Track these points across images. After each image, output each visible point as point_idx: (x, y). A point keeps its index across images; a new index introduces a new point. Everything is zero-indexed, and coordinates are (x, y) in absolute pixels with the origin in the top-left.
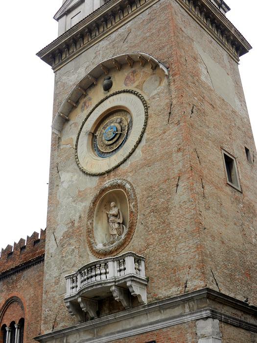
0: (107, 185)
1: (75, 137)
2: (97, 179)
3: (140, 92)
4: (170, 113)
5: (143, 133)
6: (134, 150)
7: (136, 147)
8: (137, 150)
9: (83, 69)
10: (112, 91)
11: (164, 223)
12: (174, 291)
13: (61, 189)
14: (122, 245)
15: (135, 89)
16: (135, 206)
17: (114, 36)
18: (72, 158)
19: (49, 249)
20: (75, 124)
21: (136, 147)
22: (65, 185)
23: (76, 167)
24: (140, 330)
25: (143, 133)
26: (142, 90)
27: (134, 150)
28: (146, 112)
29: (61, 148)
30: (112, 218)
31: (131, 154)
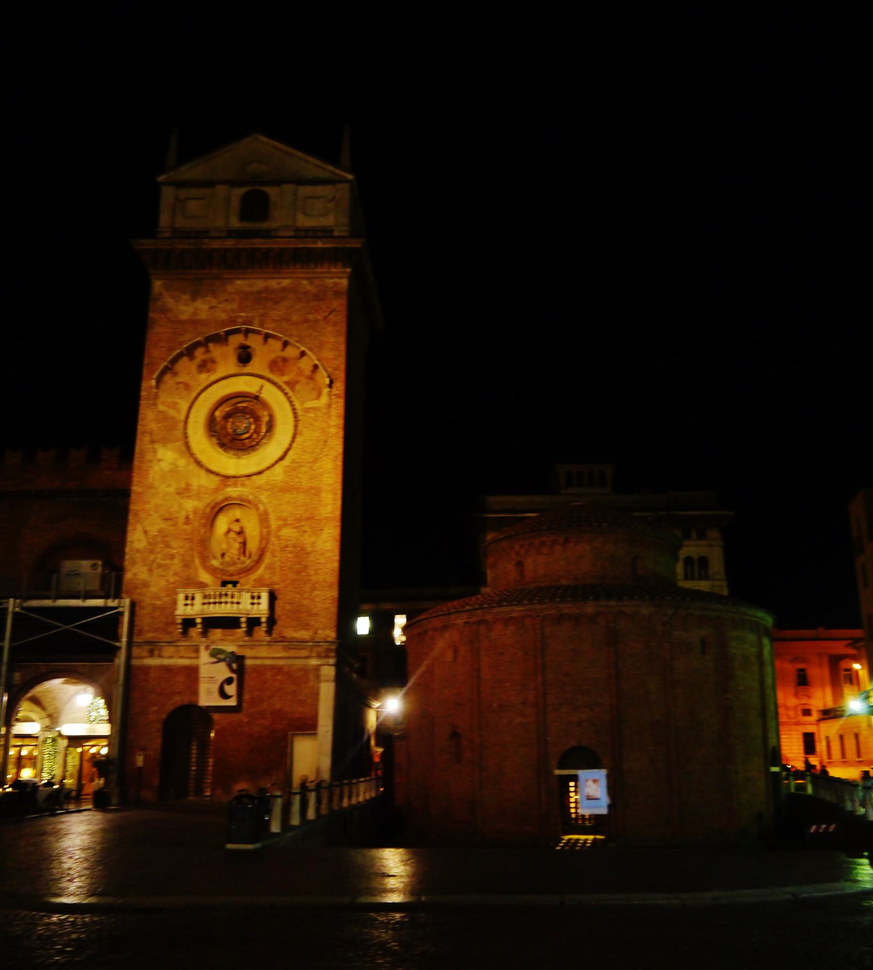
0: (234, 495)
1: (184, 405)
2: (217, 479)
3: (290, 394)
4: (326, 442)
5: (288, 450)
6: (273, 465)
7: (277, 462)
8: (277, 466)
9: (205, 307)
10: (249, 369)
11: (300, 563)
12: (304, 634)
13: (156, 468)
14: (248, 571)
15: (284, 386)
16: (269, 533)
17: (260, 284)
18: (179, 433)
19: (132, 542)
20: (187, 387)
21: (277, 462)
22: (165, 466)
23: (184, 449)
24: (258, 662)
25: (288, 450)
26: (293, 389)
27: (273, 465)
28: (296, 426)
29: (161, 408)
30: (232, 535)
31: (268, 468)
